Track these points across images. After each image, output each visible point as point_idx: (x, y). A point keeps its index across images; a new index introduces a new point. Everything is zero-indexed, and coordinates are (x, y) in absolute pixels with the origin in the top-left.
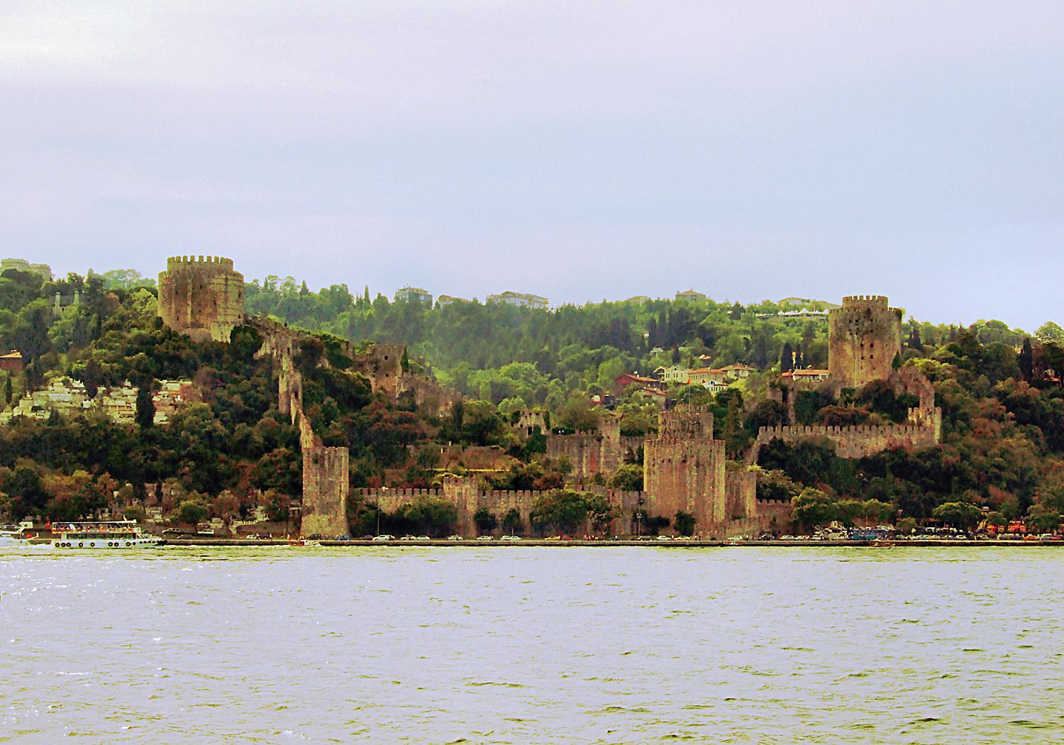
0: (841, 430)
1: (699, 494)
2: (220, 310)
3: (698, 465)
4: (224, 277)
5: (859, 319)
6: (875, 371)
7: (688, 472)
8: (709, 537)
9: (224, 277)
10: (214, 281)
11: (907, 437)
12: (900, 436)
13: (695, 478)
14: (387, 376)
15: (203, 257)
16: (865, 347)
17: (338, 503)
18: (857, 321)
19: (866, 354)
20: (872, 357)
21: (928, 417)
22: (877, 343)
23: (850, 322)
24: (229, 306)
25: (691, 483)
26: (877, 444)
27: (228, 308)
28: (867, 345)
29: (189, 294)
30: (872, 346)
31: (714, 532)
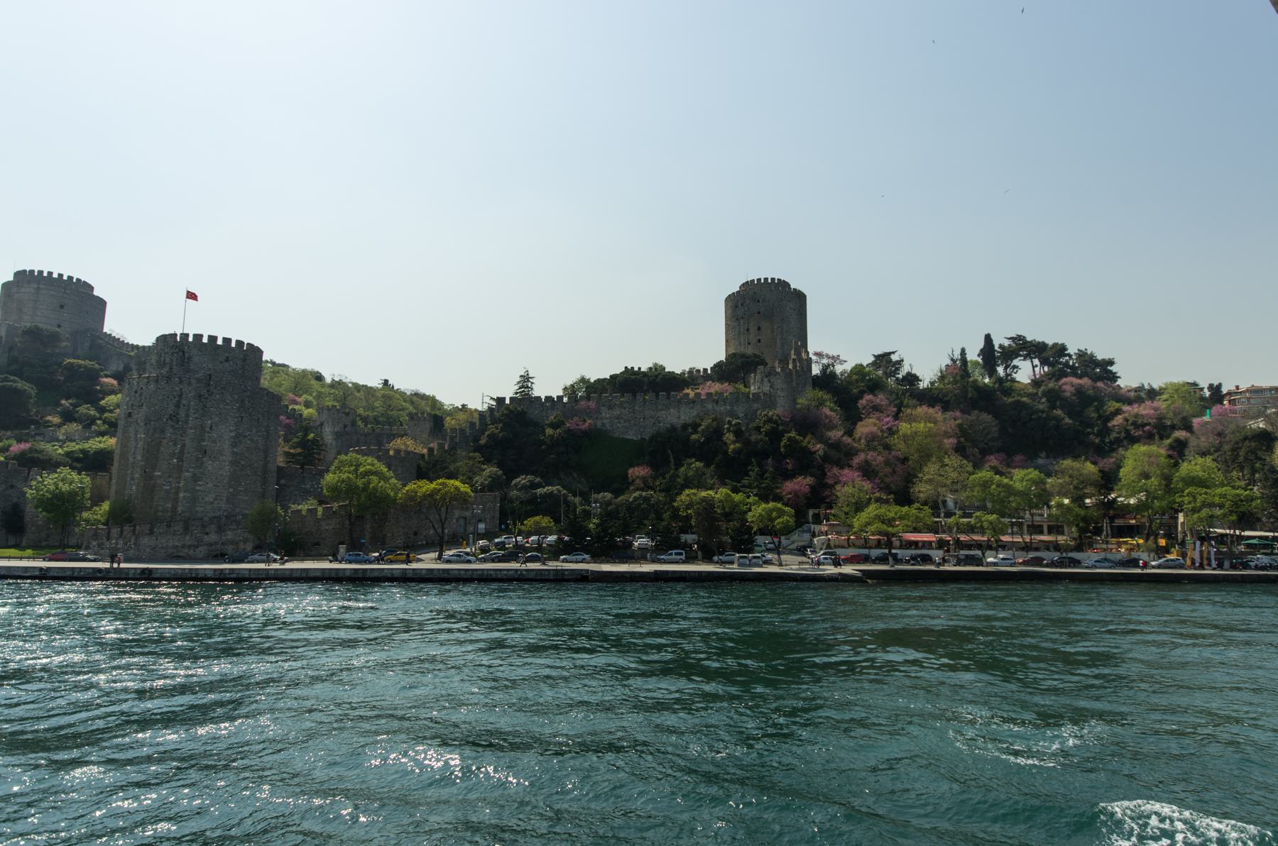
1: (147, 476)
4: (36, 286)
7: (132, 435)
9: (36, 286)
10: (23, 290)
11: (728, 407)
12: (716, 407)
16: (752, 331)
18: (742, 305)
20: (759, 341)
21: (766, 380)
23: (736, 307)
25: (134, 453)
26: (679, 418)
28: (753, 330)
30: (759, 329)
31: (117, 544)
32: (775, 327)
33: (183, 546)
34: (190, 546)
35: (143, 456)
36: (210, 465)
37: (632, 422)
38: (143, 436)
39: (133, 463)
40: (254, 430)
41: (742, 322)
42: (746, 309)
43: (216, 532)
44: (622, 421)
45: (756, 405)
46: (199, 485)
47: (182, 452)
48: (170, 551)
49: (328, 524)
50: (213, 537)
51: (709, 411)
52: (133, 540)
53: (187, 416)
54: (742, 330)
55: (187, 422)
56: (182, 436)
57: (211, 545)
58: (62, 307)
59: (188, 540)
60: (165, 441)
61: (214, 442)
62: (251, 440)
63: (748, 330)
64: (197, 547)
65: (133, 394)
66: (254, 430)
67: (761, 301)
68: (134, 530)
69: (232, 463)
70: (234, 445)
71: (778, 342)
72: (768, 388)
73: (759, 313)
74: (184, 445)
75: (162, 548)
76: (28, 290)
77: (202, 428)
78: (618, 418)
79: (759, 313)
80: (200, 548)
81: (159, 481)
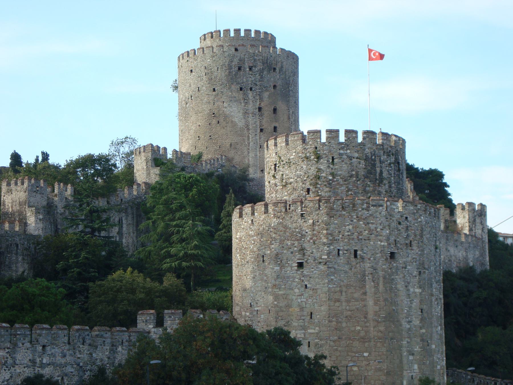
5: (255, 67)
13: (416, 303)
18: (250, 69)
20: (275, 128)
22: (281, 106)
23: (240, 69)
25: (408, 315)
30: (275, 110)
32: (291, 112)
38: (418, 290)
39: (409, 329)
41: (250, 94)
42: (258, 77)
65: (394, 224)
67: (277, 70)
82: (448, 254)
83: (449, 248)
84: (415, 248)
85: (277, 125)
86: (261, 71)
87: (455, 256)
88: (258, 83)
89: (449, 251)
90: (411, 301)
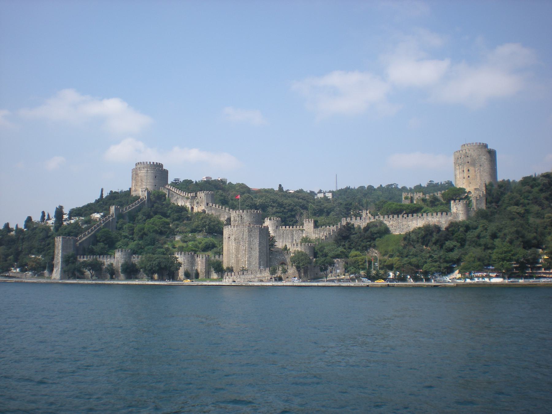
0: (393, 217)
2: (144, 183)
3: (235, 240)
4: (146, 169)
5: (461, 157)
6: (470, 185)
7: (231, 244)
8: (231, 280)
9: (146, 169)
10: (142, 172)
12: (433, 219)
14: (201, 205)
15: (147, 162)
17: (59, 262)
18: (460, 158)
19: (466, 175)
20: (469, 177)
24: (149, 182)
25: (232, 250)
26: (417, 224)
27: (148, 182)
28: (466, 171)
29: (134, 178)
30: (468, 170)
31: (234, 277)
33: (251, 278)
34: (253, 278)
35: (235, 251)
36: (253, 253)
37: (398, 227)
40: (263, 240)
41: (461, 166)
42: (462, 160)
43: (260, 274)
44: (394, 227)
45: (450, 218)
46: (251, 259)
47: (245, 249)
48: (248, 280)
49: (290, 271)
50: (259, 275)
51: (429, 221)
52: (238, 276)
53: (246, 238)
54: (460, 171)
55: (246, 240)
56: (245, 244)
57: (259, 278)
58: (156, 177)
59: (253, 276)
60: (241, 246)
61: (254, 245)
62: (263, 244)
63: (463, 171)
64: (255, 278)
66: (263, 240)
67: (469, 156)
68: (239, 273)
69: (260, 252)
70: (259, 246)
71: (478, 177)
72: (455, 210)
73: (468, 162)
74: (246, 247)
75: (246, 279)
76: (144, 171)
77: (250, 241)
78: (392, 225)
79: (468, 162)
80: (256, 279)
81: (240, 258)
82: (428, 220)
83: (428, 219)
84: (234, 235)
85: (469, 175)
86: (463, 158)
87: (432, 221)
88: (462, 162)
89: (428, 220)
90: (233, 247)
